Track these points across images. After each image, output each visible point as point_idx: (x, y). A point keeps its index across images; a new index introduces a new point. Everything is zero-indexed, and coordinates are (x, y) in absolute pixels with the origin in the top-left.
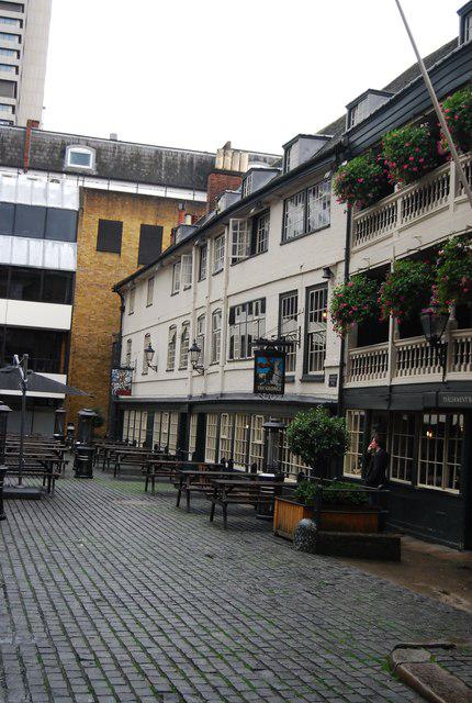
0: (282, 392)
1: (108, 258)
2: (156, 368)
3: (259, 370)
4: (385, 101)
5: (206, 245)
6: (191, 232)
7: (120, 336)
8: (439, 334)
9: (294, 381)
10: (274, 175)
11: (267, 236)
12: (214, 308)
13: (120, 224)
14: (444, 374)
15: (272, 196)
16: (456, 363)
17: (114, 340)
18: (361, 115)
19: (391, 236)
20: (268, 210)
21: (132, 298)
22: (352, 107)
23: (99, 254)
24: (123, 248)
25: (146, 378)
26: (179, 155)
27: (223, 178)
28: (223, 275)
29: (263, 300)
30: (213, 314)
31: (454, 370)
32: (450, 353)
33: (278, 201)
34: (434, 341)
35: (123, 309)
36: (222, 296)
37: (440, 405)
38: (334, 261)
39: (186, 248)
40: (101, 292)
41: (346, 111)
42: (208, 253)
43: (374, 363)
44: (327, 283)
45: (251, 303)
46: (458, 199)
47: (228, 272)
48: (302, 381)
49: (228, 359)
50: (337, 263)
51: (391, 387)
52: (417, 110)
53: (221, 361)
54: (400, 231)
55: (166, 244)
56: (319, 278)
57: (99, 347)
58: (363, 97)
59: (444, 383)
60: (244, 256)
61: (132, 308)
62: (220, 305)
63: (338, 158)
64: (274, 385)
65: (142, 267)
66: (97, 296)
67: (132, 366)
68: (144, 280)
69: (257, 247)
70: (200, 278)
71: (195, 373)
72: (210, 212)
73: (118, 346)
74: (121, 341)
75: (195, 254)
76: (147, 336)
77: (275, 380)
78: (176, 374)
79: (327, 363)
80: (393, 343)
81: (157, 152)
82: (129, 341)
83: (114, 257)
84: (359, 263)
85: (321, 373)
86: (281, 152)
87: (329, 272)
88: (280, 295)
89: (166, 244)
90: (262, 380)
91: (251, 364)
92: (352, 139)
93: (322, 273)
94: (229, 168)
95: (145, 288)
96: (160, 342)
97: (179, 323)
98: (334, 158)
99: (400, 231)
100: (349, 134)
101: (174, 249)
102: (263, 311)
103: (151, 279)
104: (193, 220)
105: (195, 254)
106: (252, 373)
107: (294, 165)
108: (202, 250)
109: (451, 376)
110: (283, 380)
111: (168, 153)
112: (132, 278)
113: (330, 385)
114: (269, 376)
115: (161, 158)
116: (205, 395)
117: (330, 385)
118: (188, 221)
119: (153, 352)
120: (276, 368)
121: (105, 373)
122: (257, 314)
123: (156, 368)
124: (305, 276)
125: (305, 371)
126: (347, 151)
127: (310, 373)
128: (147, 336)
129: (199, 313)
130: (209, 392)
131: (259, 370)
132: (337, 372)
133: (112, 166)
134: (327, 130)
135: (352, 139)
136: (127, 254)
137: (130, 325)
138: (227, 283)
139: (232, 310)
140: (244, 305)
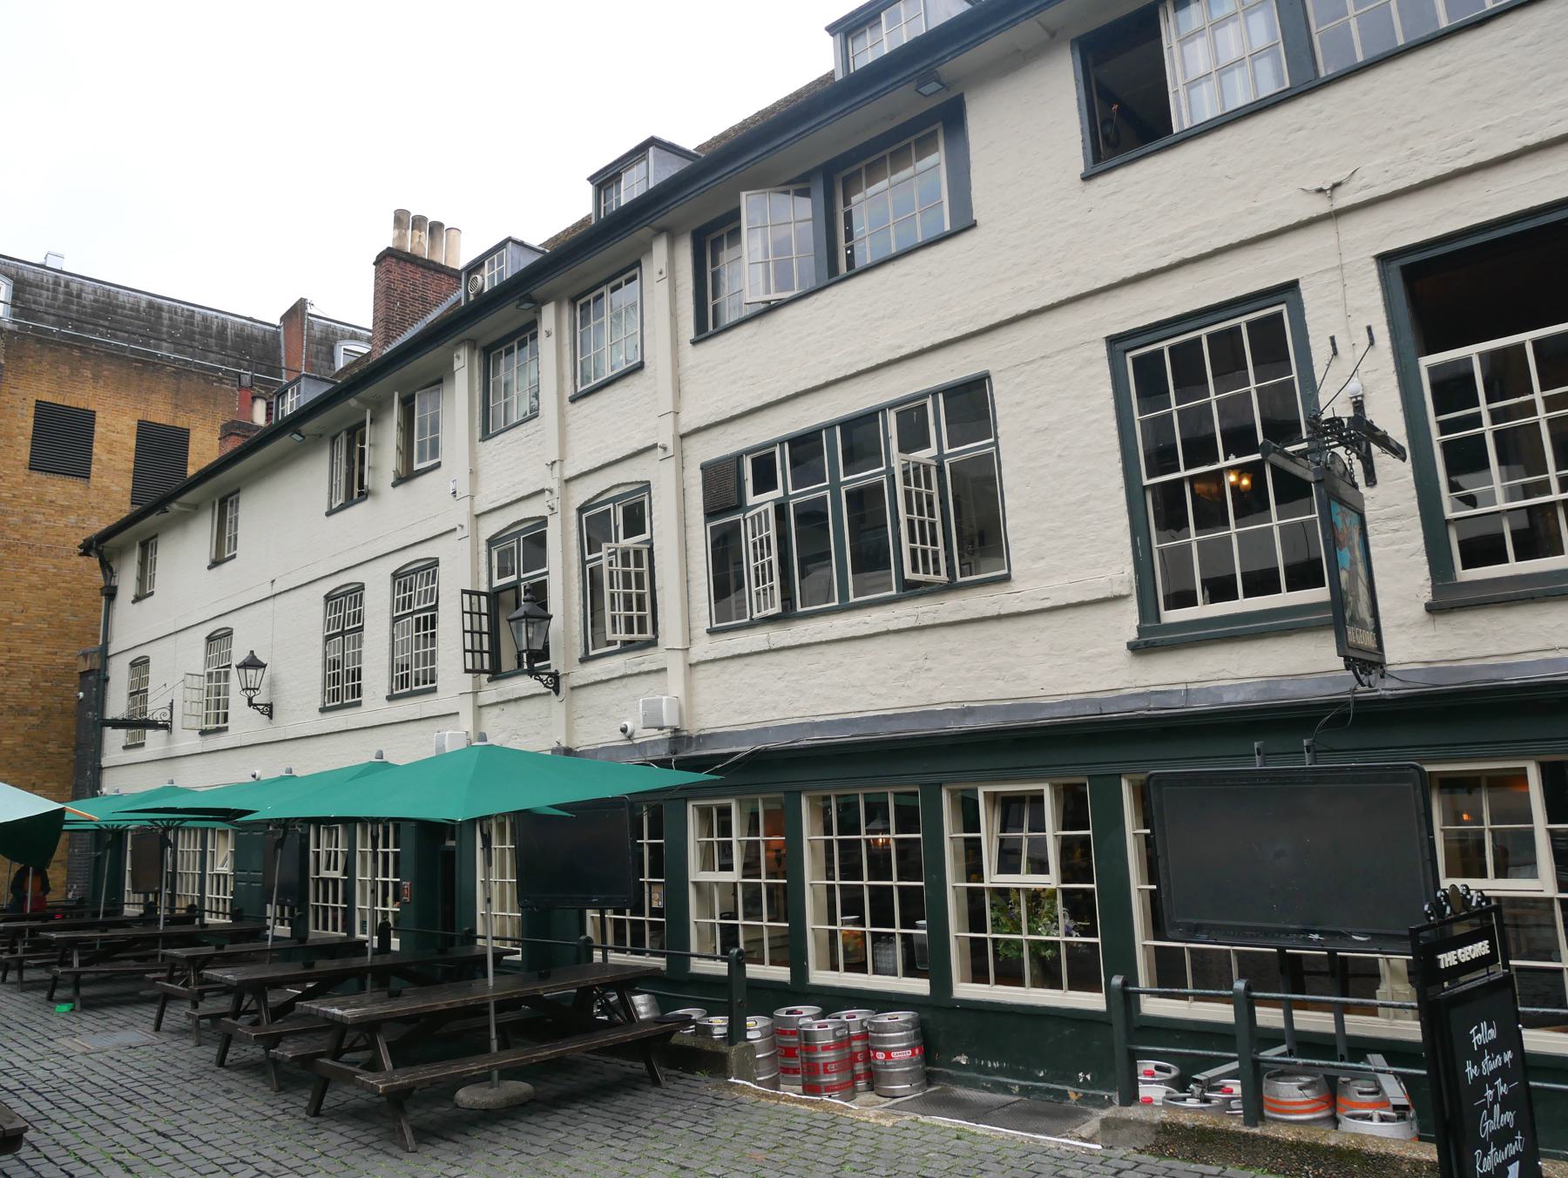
1: (58, 488)
2: (269, 710)
7: (105, 657)
17: (84, 666)
23: (37, 476)
24: (94, 468)
26: (198, 318)
35: (110, 593)
36: (666, 438)
40: (40, 563)
48: (1432, 609)
57: (36, 687)
66: (33, 570)
70: (486, 435)
73: (96, 679)
74: (105, 667)
75: (464, 368)
76: (219, 639)
81: (151, 305)
82: (141, 665)
83: (73, 487)
88: (1112, 341)
105: (464, 368)
121: (52, 747)
123: (269, 710)
128: (219, 639)
136: (106, 481)
139: (713, 472)
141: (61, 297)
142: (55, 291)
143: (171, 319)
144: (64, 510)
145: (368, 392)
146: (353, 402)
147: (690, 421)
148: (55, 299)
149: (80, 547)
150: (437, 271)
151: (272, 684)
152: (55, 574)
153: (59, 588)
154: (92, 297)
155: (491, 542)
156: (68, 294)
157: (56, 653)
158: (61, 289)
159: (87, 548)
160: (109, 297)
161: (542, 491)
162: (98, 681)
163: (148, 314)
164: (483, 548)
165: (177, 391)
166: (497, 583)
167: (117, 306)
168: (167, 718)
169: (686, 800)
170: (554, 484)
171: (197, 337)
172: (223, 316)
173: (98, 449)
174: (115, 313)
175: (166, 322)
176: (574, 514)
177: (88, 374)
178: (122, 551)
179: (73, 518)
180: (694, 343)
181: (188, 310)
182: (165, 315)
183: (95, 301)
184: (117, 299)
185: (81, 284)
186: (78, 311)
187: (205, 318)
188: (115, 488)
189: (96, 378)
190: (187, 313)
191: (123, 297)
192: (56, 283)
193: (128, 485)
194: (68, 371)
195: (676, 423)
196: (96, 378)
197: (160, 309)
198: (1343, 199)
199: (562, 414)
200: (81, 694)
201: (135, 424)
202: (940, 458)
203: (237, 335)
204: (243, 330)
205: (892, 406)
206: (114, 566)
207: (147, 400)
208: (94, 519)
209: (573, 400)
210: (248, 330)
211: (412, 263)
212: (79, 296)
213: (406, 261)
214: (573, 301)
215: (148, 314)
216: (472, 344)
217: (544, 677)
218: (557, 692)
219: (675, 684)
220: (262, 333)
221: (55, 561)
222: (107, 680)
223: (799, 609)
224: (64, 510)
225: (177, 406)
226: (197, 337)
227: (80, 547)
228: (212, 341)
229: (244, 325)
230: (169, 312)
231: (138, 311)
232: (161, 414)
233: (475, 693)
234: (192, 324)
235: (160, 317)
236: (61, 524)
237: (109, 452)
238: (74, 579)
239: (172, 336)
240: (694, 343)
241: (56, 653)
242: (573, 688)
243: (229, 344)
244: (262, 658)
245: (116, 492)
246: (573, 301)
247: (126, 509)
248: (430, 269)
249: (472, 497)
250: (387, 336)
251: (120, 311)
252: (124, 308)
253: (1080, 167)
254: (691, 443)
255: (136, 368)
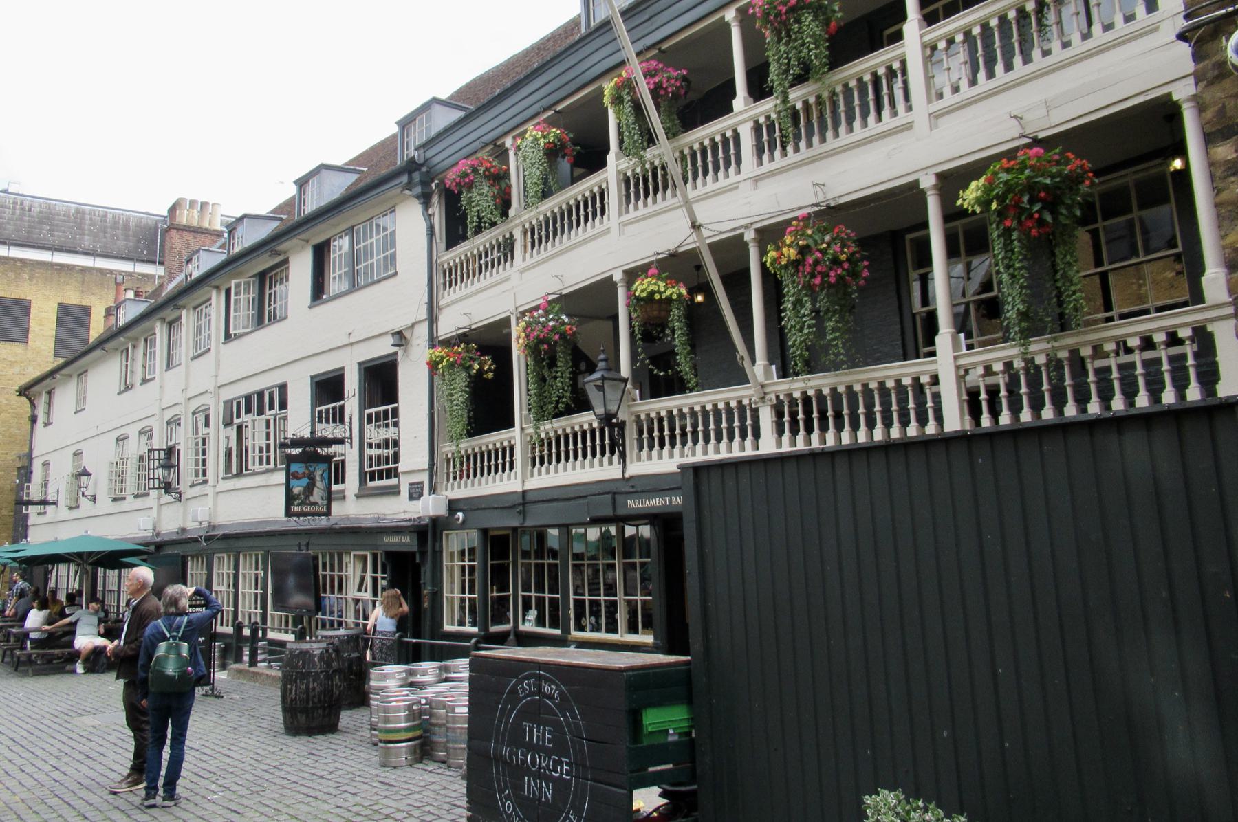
0: (328, 513)
2: (94, 498)
3: (293, 482)
4: (460, 114)
5: (179, 318)
6: (141, 308)
7: (30, 457)
8: (613, 408)
9: (344, 497)
10: (275, 224)
11: (287, 297)
12: (194, 405)
13: (29, 302)
14: (624, 466)
15: (294, 241)
16: (641, 448)
18: (418, 136)
19: (508, 279)
20: (286, 261)
21: (49, 404)
22: (405, 124)
24: (30, 336)
25: (75, 514)
26: (110, 216)
27: (190, 237)
28: (209, 359)
29: (283, 388)
30: (194, 413)
31: (639, 459)
32: (631, 434)
33: (303, 248)
34: (607, 419)
35: (34, 420)
37: (621, 512)
38: (409, 323)
39: (146, 325)
41: (395, 129)
42: (184, 329)
43: (502, 460)
44: (396, 353)
45: (260, 394)
46: (626, 217)
47: (218, 353)
48: (358, 496)
49: (222, 474)
50: (413, 325)
51: (524, 492)
52: (545, 103)
53: (210, 476)
54: (522, 272)
55: (97, 328)
56: (383, 348)
58: (426, 107)
59: (624, 480)
60: (242, 331)
61: (48, 414)
62: (208, 400)
63: (410, 179)
64: (315, 504)
65: (61, 361)
67: (50, 498)
68: (70, 376)
69: (263, 316)
71: (167, 498)
72: (170, 282)
73: (25, 473)
75: (160, 330)
76: (77, 454)
77: (317, 495)
78: (130, 503)
79: (402, 466)
80: (522, 429)
81: (77, 211)
82: (46, 464)
83: (17, 349)
84: (449, 325)
85: (393, 481)
86: (293, 190)
87: (401, 337)
89: (97, 328)
90: (298, 497)
91: (281, 477)
92: (429, 154)
93: (390, 340)
94: (195, 224)
95: (73, 384)
96: (99, 459)
97: (133, 431)
98: (405, 179)
99: (522, 272)
100: (425, 146)
101: (101, 343)
102: (283, 405)
103: (82, 374)
104: (137, 294)
105: (160, 330)
106: (283, 489)
107: (310, 207)
108: (172, 325)
109: (635, 469)
110: (329, 497)
111: (93, 213)
112: (52, 373)
113: (411, 498)
114: (309, 490)
115: (83, 219)
116: (184, 530)
117: (411, 498)
118: (131, 294)
119: (89, 475)
120: (318, 478)
122: (271, 408)
123: (94, 498)
124: (355, 347)
125: (362, 481)
126: (424, 169)
127: (371, 484)
128: (77, 454)
129: (168, 415)
130: (190, 525)
131: (293, 482)
132: (425, 478)
133: (11, 228)
134: (358, 160)
135: (429, 154)
137: (44, 440)
138: (218, 365)
139: (228, 404)
140: (248, 398)
141: (18, 212)
142: (14, 208)
143: (91, 219)
144: (12, 364)
145: (130, 334)
146: (122, 339)
147: (221, 381)
148: (13, 214)
149: (17, 391)
150: (203, 233)
151: (96, 484)
152: (6, 405)
153: (9, 413)
154: (38, 210)
155: (168, 423)
156: (23, 209)
157: (7, 454)
158: (18, 207)
159: (24, 391)
160: (49, 208)
161: (177, 404)
162: (27, 473)
163: (76, 217)
164: (165, 424)
165: (83, 282)
166: (170, 444)
167: (54, 215)
168: (56, 498)
169: (214, 554)
170: (182, 401)
171: (109, 230)
172: (127, 213)
173: (32, 324)
174: (54, 219)
175: (88, 222)
176: (191, 415)
177: (26, 276)
178: (40, 394)
179: (17, 369)
180: (224, 343)
181: (103, 212)
182: (88, 217)
183: (40, 212)
184: (55, 209)
185: (31, 201)
186: (29, 221)
187: (114, 217)
188: (43, 348)
189: (31, 278)
190: (102, 214)
191: (59, 207)
192: (15, 203)
193: (51, 344)
194: (13, 276)
195: (216, 382)
196: (31, 278)
197: (84, 213)
198: (352, 340)
199: (187, 367)
200: (17, 481)
201: (56, 305)
202: (275, 416)
203: (136, 226)
204: (141, 222)
205: (267, 389)
206: (36, 402)
207: (63, 290)
208: (31, 368)
209: (193, 358)
210: (144, 222)
211: (186, 231)
212: (30, 210)
213: (182, 230)
214: (195, 308)
215: (76, 217)
216: (163, 320)
217: (173, 494)
218: (180, 501)
219: (210, 501)
220: (154, 223)
221: (6, 396)
222: (31, 473)
223: (244, 472)
224: (12, 364)
225: (83, 292)
226: (109, 230)
227: (17, 391)
228: (119, 232)
229: (142, 218)
230: (90, 214)
231: (69, 216)
232: (73, 297)
233: (158, 498)
234: (105, 221)
235: (84, 219)
236: (10, 373)
237: (40, 325)
238: (18, 407)
239: (91, 231)
240: (224, 343)
241: (7, 454)
242: (187, 499)
243: (131, 233)
244: (89, 470)
245: (44, 350)
246: (195, 308)
247: (51, 363)
248: (198, 232)
249: (161, 400)
250: (170, 277)
251: (56, 217)
252: (59, 215)
253: (309, 304)
254: (222, 391)
255: (56, 269)
